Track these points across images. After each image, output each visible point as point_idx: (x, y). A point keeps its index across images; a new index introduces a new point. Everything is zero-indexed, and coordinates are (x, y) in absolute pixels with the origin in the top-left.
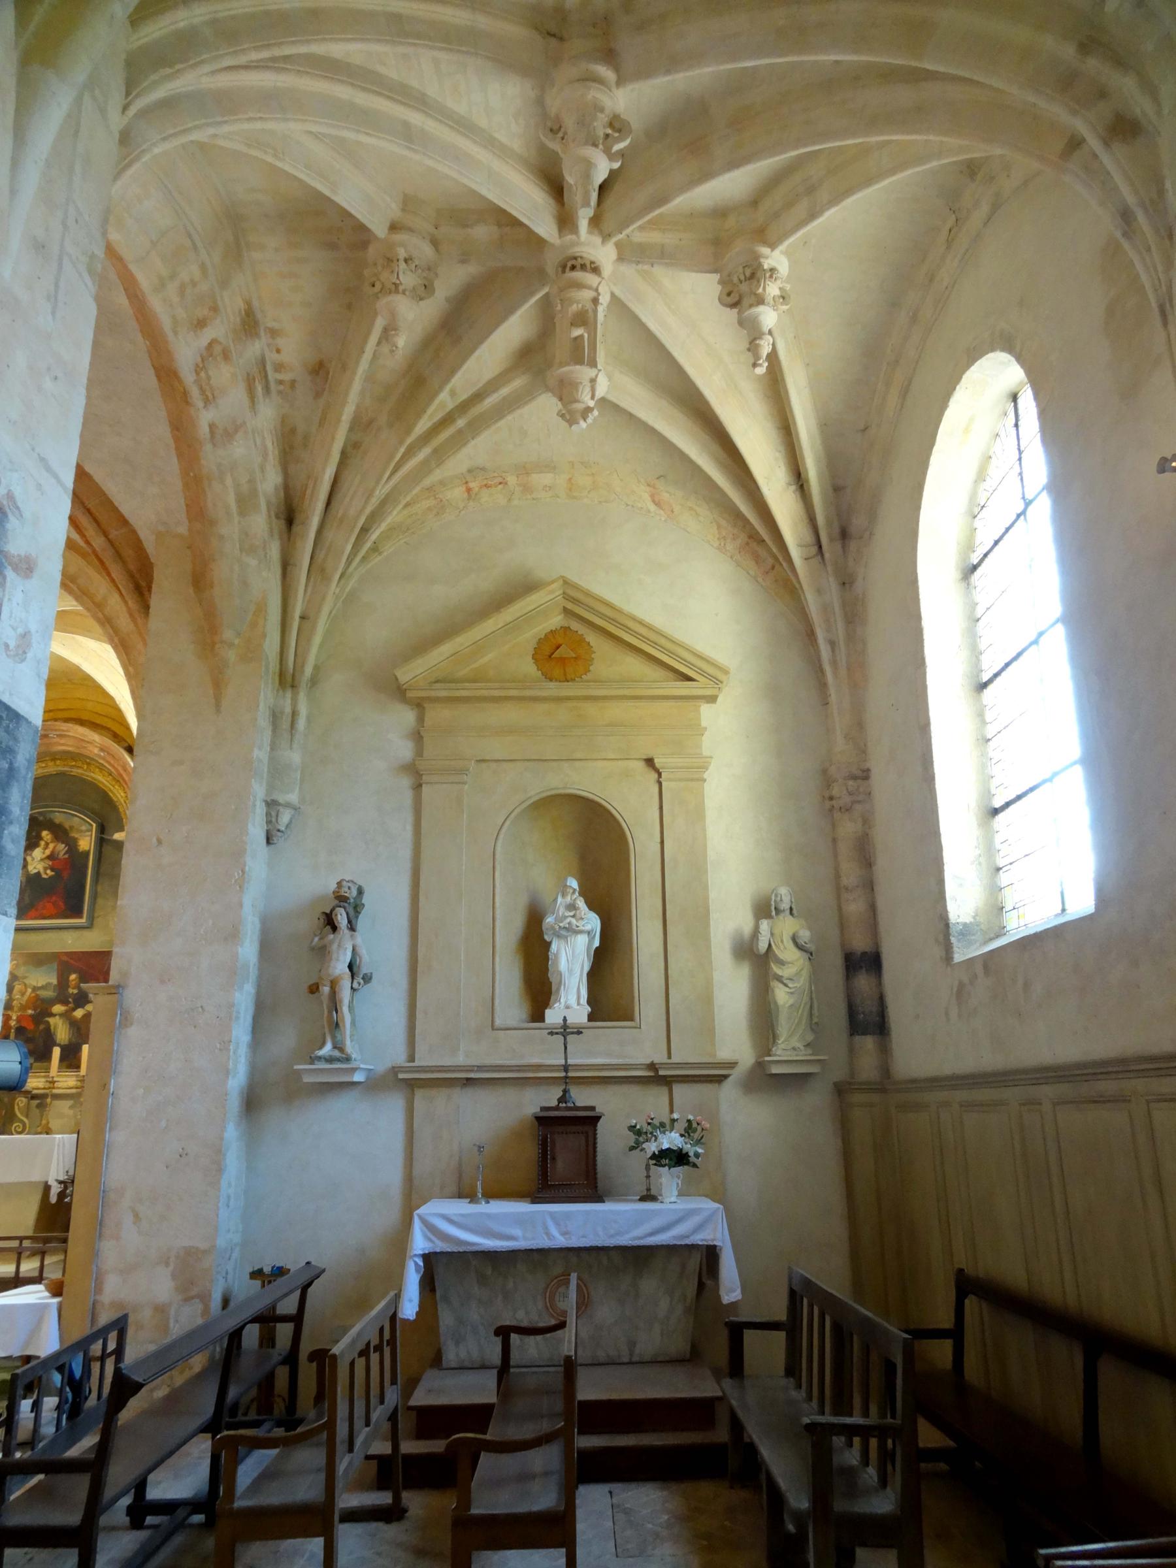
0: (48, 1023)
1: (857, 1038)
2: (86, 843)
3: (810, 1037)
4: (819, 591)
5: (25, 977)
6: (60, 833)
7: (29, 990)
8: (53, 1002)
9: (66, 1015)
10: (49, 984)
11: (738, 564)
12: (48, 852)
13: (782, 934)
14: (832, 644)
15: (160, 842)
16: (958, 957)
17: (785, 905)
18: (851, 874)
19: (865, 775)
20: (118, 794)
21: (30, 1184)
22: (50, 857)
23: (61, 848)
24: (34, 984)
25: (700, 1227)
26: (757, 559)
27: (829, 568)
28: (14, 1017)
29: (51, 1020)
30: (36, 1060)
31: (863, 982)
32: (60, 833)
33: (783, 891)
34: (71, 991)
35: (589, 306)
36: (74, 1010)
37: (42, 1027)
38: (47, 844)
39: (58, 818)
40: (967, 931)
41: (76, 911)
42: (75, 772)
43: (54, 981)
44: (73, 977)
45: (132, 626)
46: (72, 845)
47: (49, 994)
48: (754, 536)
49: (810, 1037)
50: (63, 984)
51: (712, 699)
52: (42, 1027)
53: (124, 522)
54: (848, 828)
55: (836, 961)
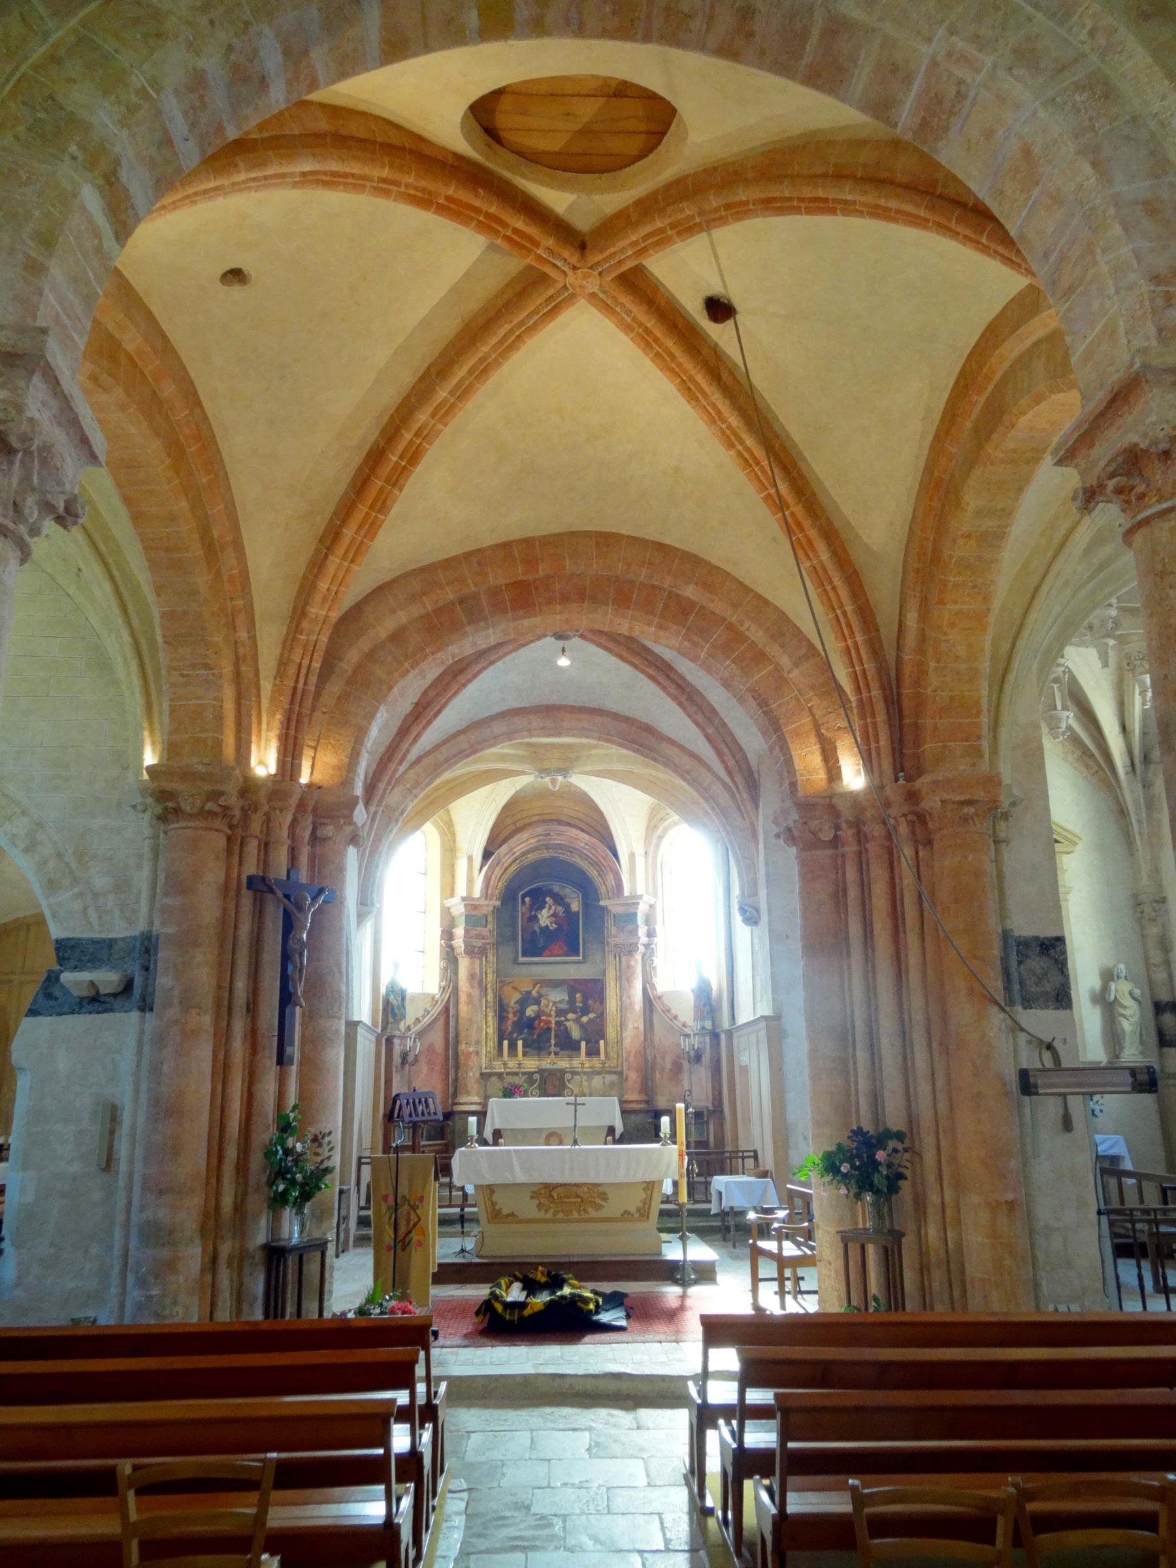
1: (1166, 1050)
2: (575, 906)
3: (1141, 1048)
4: (1132, 792)
6: (559, 899)
11: (1075, 768)
12: (551, 912)
13: (1122, 990)
14: (1139, 821)
15: (787, 937)
17: (1123, 975)
18: (1156, 957)
19: (1163, 900)
20: (592, 872)
21: (600, 1127)
22: (554, 915)
23: (560, 909)
25: (1111, 1147)
26: (1087, 766)
27: (1139, 778)
29: (568, 1024)
30: (561, 1049)
32: (559, 899)
33: (1122, 966)
35: (1061, 675)
38: (550, 908)
42: (562, 857)
44: (578, 995)
45: (730, 803)
46: (567, 907)
47: (564, 1006)
48: (1086, 752)
49: (1141, 1048)
50: (572, 1000)
51: (1069, 853)
53: (741, 749)
54: (1153, 931)
55: (1149, 1007)
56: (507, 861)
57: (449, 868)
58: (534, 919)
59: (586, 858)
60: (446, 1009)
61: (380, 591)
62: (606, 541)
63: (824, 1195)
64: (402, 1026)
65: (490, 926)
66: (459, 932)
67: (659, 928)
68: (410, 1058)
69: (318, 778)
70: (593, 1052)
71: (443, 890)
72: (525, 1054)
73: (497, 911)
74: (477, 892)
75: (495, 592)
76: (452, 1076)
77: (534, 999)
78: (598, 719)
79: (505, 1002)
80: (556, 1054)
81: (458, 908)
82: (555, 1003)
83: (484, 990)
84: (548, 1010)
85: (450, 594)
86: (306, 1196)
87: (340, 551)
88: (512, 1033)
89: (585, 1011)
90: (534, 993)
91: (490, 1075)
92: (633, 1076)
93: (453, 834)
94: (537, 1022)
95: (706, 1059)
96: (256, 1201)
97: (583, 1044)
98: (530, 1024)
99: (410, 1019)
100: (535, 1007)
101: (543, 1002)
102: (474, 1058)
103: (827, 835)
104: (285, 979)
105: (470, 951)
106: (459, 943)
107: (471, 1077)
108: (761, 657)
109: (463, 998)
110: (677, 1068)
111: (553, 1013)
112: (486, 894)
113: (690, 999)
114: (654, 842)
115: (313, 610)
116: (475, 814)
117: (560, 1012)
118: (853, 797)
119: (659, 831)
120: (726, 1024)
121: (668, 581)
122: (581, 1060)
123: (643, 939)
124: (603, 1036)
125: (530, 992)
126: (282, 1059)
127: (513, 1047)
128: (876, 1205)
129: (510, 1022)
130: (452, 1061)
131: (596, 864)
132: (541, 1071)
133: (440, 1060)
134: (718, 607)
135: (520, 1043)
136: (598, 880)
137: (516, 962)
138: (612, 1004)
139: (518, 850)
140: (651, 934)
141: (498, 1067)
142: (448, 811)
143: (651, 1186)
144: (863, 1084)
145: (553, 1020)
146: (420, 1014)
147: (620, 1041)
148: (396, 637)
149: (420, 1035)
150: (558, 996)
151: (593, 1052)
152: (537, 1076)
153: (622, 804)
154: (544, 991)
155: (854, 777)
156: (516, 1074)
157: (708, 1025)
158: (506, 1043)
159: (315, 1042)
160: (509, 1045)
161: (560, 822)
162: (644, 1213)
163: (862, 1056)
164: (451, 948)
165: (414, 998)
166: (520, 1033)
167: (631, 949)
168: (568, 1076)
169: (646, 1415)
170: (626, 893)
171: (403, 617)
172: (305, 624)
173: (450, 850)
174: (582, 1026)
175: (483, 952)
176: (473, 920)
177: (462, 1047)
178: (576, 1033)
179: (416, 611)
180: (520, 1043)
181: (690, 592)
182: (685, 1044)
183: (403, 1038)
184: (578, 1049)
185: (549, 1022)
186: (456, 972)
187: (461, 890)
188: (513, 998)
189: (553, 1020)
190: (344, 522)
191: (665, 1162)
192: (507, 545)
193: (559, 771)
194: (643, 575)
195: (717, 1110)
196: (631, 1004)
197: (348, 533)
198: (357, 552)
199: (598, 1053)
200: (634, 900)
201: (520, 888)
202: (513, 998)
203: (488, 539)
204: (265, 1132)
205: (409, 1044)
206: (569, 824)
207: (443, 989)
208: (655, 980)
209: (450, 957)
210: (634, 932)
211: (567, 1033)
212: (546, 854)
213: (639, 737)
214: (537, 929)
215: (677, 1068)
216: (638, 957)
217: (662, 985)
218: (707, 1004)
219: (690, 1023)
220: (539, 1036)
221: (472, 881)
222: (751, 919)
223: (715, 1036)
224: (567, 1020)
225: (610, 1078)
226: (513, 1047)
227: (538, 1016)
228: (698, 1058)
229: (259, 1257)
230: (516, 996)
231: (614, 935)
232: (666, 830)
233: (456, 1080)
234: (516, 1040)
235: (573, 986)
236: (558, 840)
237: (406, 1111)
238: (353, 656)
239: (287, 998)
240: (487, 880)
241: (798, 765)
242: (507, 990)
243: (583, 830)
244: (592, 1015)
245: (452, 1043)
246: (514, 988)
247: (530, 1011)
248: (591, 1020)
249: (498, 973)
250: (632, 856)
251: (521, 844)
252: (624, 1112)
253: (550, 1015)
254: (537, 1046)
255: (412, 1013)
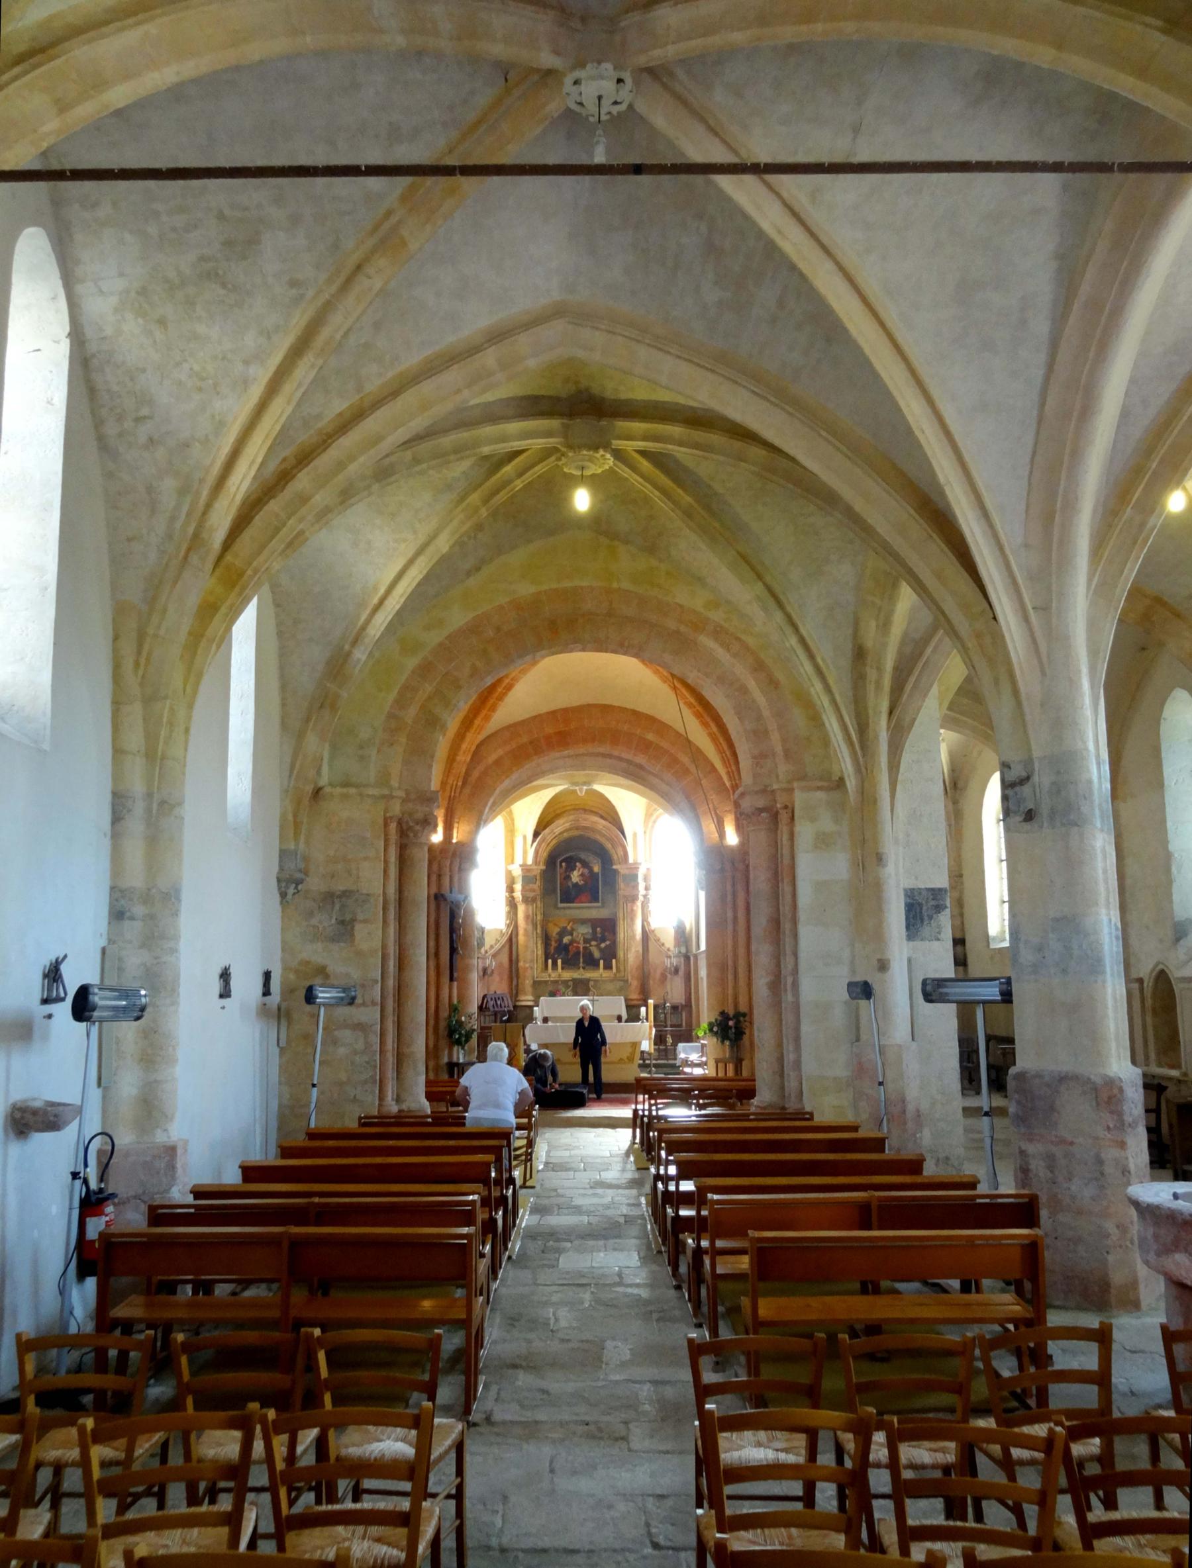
2: (596, 869)
6: (585, 864)
9: (598, 946)
16: (992, 946)
19: (961, 876)
20: (608, 846)
21: (612, 1016)
22: (582, 875)
23: (586, 871)
31: (959, 948)
32: (585, 864)
39: (583, 856)
40: (994, 938)
41: (596, 899)
46: (591, 870)
47: (589, 937)
50: (594, 932)
56: (549, 838)
57: (510, 844)
58: (568, 878)
59: (604, 836)
60: (510, 940)
61: (489, 737)
62: (606, 709)
63: (709, 1041)
64: (483, 951)
65: (538, 883)
66: (518, 887)
67: (653, 885)
68: (489, 972)
69: (461, 838)
70: (608, 967)
71: (506, 858)
73: (544, 872)
74: (530, 861)
75: (548, 738)
76: (514, 983)
78: (608, 760)
81: (517, 872)
83: (535, 926)
85: (525, 739)
86: (467, 1041)
87: (473, 731)
89: (603, 940)
91: (540, 982)
92: (635, 984)
93: (513, 820)
95: (681, 972)
96: (443, 1043)
97: (602, 962)
99: (487, 946)
100: (569, 937)
102: (529, 971)
103: (718, 867)
104: (452, 941)
105: (526, 900)
106: (518, 895)
107: (528, 983)
108: (687, 771)
109: (521, 932)
110: (664, 978)
112: (536, 861)
113: (672, 932)
114: (650, 824)
115: (458, 758)
116: (528, 809)
117: (586, 941)
118: (731, 849)
119: (654, 818)
120: (694, 951)
121: (638, 731)
122: (600, 973)
123: (642, 891)
124: (615, 957)
126: (451, 979)
127: (555, 964)
128: (732, 1046)
130: (513, 971)
131: (609, 839)
132: (574, 980)
133: (506, 972)
134: (665, 744)
135: (559, 961)
136: (612, 851)
137: (557, 908)
138: (621, 935)
139: (558, 830)
140: (647, 888)
141: (544, 977)
142: (511, 813)
143: (635, 1045)
144: (730, 991)
145: (581, 946)
146: (493, 942)
147: (626, 960)
148: (498, 763)
149: (494, 956)
150: (584, 930)
151: (608, 967)
152: (571, 983)
153: (628, 802)
154: (575, 926)
155: (732, 838)
156: (556, 982)
157: (683, 950)
159: (467, 969)
161: (585, 810)
162: (631, 1059)
163: (730, 977)
164: (513, 898)
165: (490, 931)
167: (634, 898)
168: (591, 983)
169: (619, 1130)
170: (631, 861)
171: (500, 752)
172: (455, 765)
173: (511, 831)
174: (601, 950)
175: (534, 900)
176: (527, 879)
177: (521, 964)
178: (597, 954)
179: (508, 748)
180: (559, 961)
181: (650, 737)
182: (668, 962)
183: (484, 958)
184: (598, 965)
185: (578, 948)
186: (516, 914)
187: (519, 860)
188: (554, 931)
189: (581, 946)
190: (475, 716)
191: (644, 1036)
192: (554, 712)
193: (585, 783)
194: (626, 727)
195: (688, 1005)
196: (634, 936)
197: (477, 722)
198: (481, 728)
199: (611, 968)
200: (635, 867)
201: (559, 855)
202: (554, 931)
203: (544, 709)
204: (444, 1014)
205: (488, 962)
206: (592, 812)
207: (508, 926)
208: (650, 920)
209: (512, 904)
210: (636, 887)
211: (591, 954)
212: (576, 833)
213: (636, 775)
214: (570, 884)
215: (664, 978)
216: (639, 903)
217: (655, 923)
218: (682, 936)
219: (672, 948)
221: (526, 853)
222: (702, 889)
223: (687, 958)
225: (622, 983)
226: (555, 964)
227: (571, 942)
228: (676, 971)
229: (445, 1068)
230: (557, 930)
231: (623, 889)
232: (657, 817)
233: (517, 985)
235: (594, 923)
236: (585, 824)
237: (491, 1003)
238: (476, 774)
239: (453, 950)
240: (537, 852)
241: (705, 830)
242: (550, 925)
243: (602, 817)
245: (513, 961)
247: (566, 940)
249: (545, 915)
250: (635, 835)
251: (560, 827)
252: (627, 1007)
254: (570, 963)
255: (489, 941)
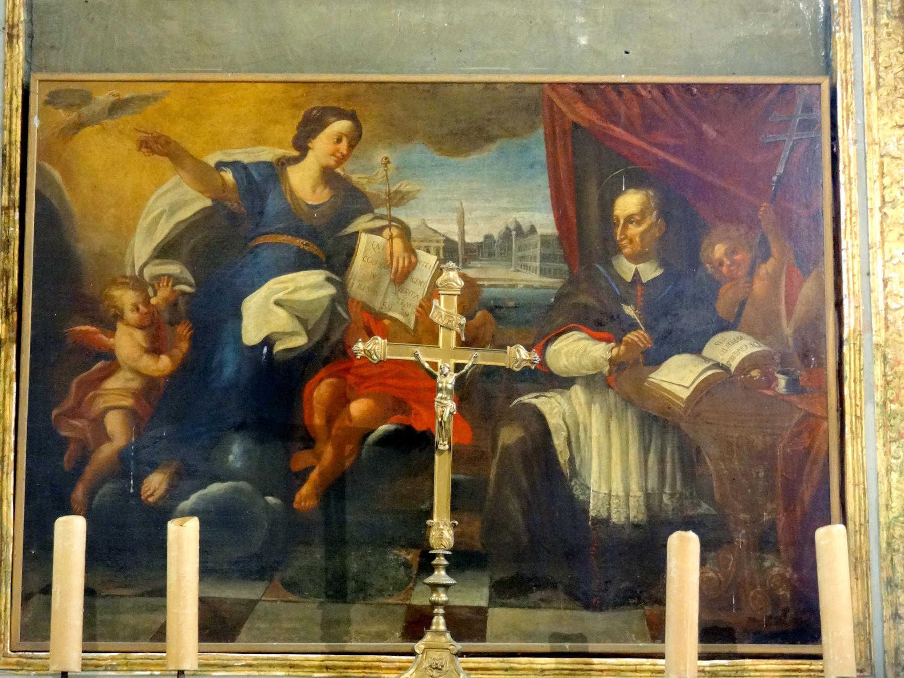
0: (541, 417)
5: (398, 199)
7: (428, 260)
8: (544, 322)
9: (620, 383)
10: (519, 232)
24: (450, 229)
28: (448, 381)
29: (553, 407)
30: (509, 590)
34: (626, 268)
36: (655, 358)
37: (509, 436)
43: (545, 222)
44: (629, 202)
47: (526, 279)
50: (583, 238)
52: (509, 436)
72: (217, 626)
77: (296, 221)
79: (89, 240)
80: (467, 626)
82: (451, 251)
84: (401, 308)
88: (132, 466)
90: (303, 182)
94: (321, 391)
97: (684, 553)
98: (276, 389)
100: (310, 286)
101: (370, 247)
111: (445, 311)
117: (489, 321)
125: (274, 172)
129: (118, 389)
135: (184, 537)
145: (446, 361)
150: (483, 208)
158: (71, 534)
160: (96, 553)
166: (186, 478)
174: (657, 422)
178: (611, 474)
180: (184, 537)
184: (642, 587)
188: (143, 215)
189: (446, 361)
202: (143, 215)
220: (335, 490)
224: (546, 379)
227: (328, 348)
230: (174, 201)
234: (159, 517)
244: (733, 349)
246: (157, 145)
247: (273, 311)
248: (718, 385)
253: (426, 332)
